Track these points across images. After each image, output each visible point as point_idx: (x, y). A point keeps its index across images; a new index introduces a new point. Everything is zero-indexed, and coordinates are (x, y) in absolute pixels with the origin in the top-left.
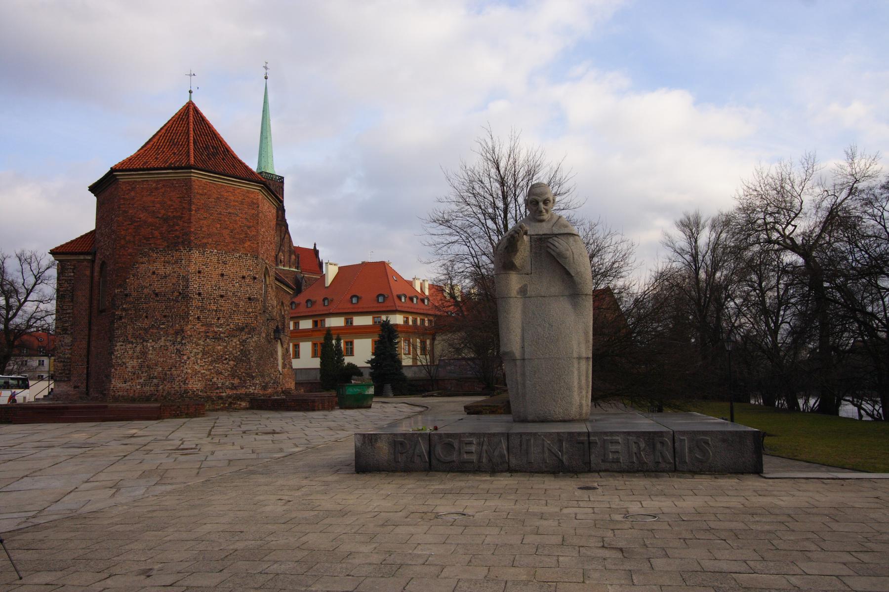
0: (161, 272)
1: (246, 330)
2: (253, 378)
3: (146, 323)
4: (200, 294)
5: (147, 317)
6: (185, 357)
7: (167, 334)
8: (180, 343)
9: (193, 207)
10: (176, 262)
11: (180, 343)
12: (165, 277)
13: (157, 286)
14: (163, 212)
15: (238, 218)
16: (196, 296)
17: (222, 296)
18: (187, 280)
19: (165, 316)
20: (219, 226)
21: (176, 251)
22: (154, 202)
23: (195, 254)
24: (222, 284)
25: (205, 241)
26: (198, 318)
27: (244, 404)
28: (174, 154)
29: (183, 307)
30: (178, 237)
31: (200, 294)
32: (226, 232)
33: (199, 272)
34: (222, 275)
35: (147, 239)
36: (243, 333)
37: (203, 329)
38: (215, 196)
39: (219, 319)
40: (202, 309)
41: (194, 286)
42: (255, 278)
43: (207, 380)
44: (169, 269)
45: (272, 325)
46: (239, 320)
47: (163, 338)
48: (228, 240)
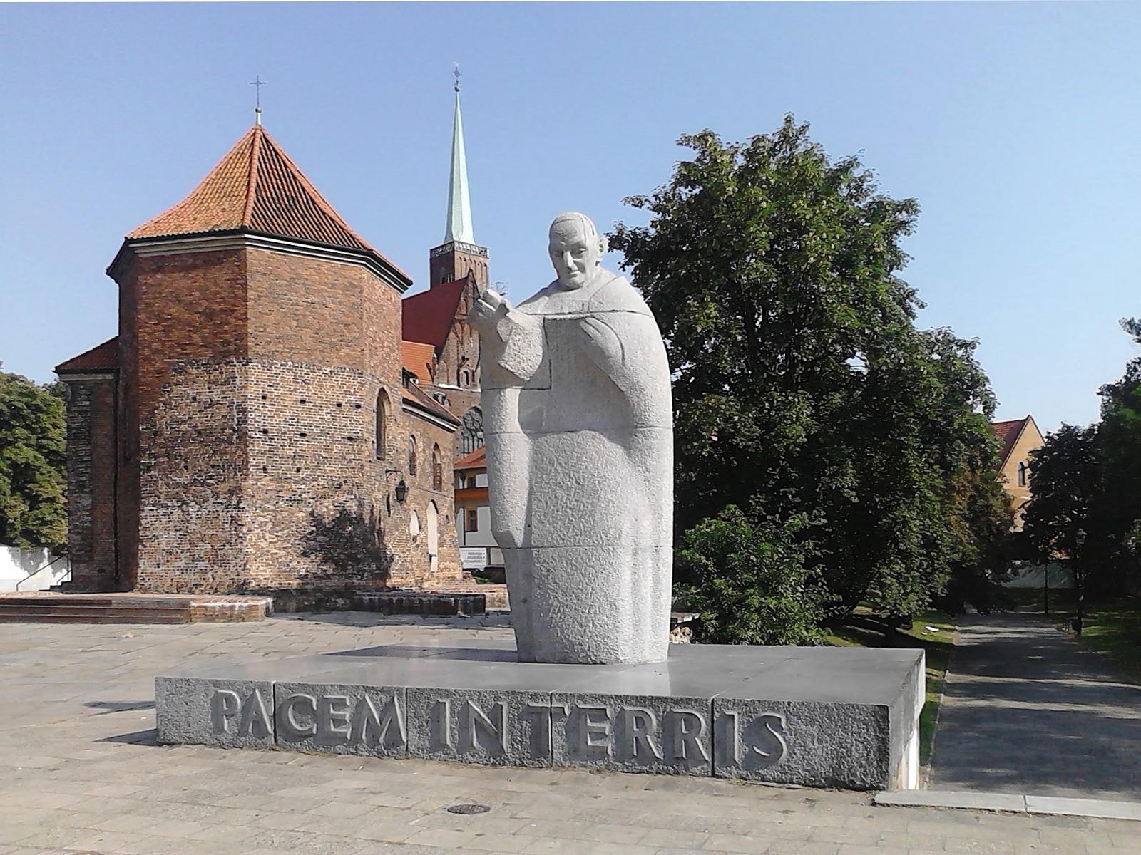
0: (205, 398)
1: (344, 487)
2: (358, 561)
3: (185, 477)
4: (265, 432)
5: (186, 467)
6: (245, 530)
7: (217, 495)
8: (237, 507)
9: (251, 294)
10: (226, 383)
11: (237, 507)
12: (211, 406)
13: (201, 421)
14: (204, 303)
15: (326, 311)
16: (262, 435)
17: (303, 435)
18: (244, 411)
19: (213, 466)
20: (295, 324)
21: (227, 364)
22: (190, 288)
23: (256, 371)
24: (302, 416)
25: (272, 347)
26: (265, 469)
27: (341, 601)
28: (224, 210)
29: (239, 453)
30: (229, 343)
31: (265, 432)
32: (307, 334)
33: (264, 397)
34: (303, 402)
35: (183, 347)
36: (339, 492)
37: (273, 486)
38: (287, 276)
39: (298, 470)
40: (271, 455)
41: (255, 420)
42: (358, 407)
43: (280, 564)
44: (217, 391)
45: (394, 481)
46: (333, 471)
47: (212, 500)
48: (310, 343)
